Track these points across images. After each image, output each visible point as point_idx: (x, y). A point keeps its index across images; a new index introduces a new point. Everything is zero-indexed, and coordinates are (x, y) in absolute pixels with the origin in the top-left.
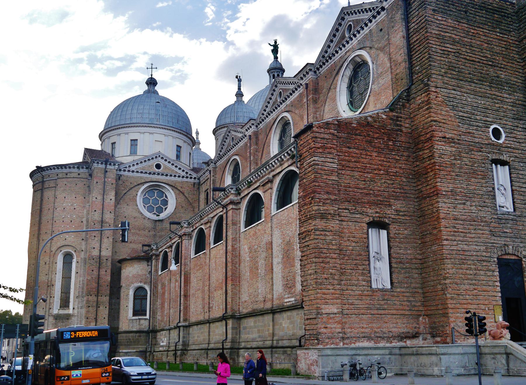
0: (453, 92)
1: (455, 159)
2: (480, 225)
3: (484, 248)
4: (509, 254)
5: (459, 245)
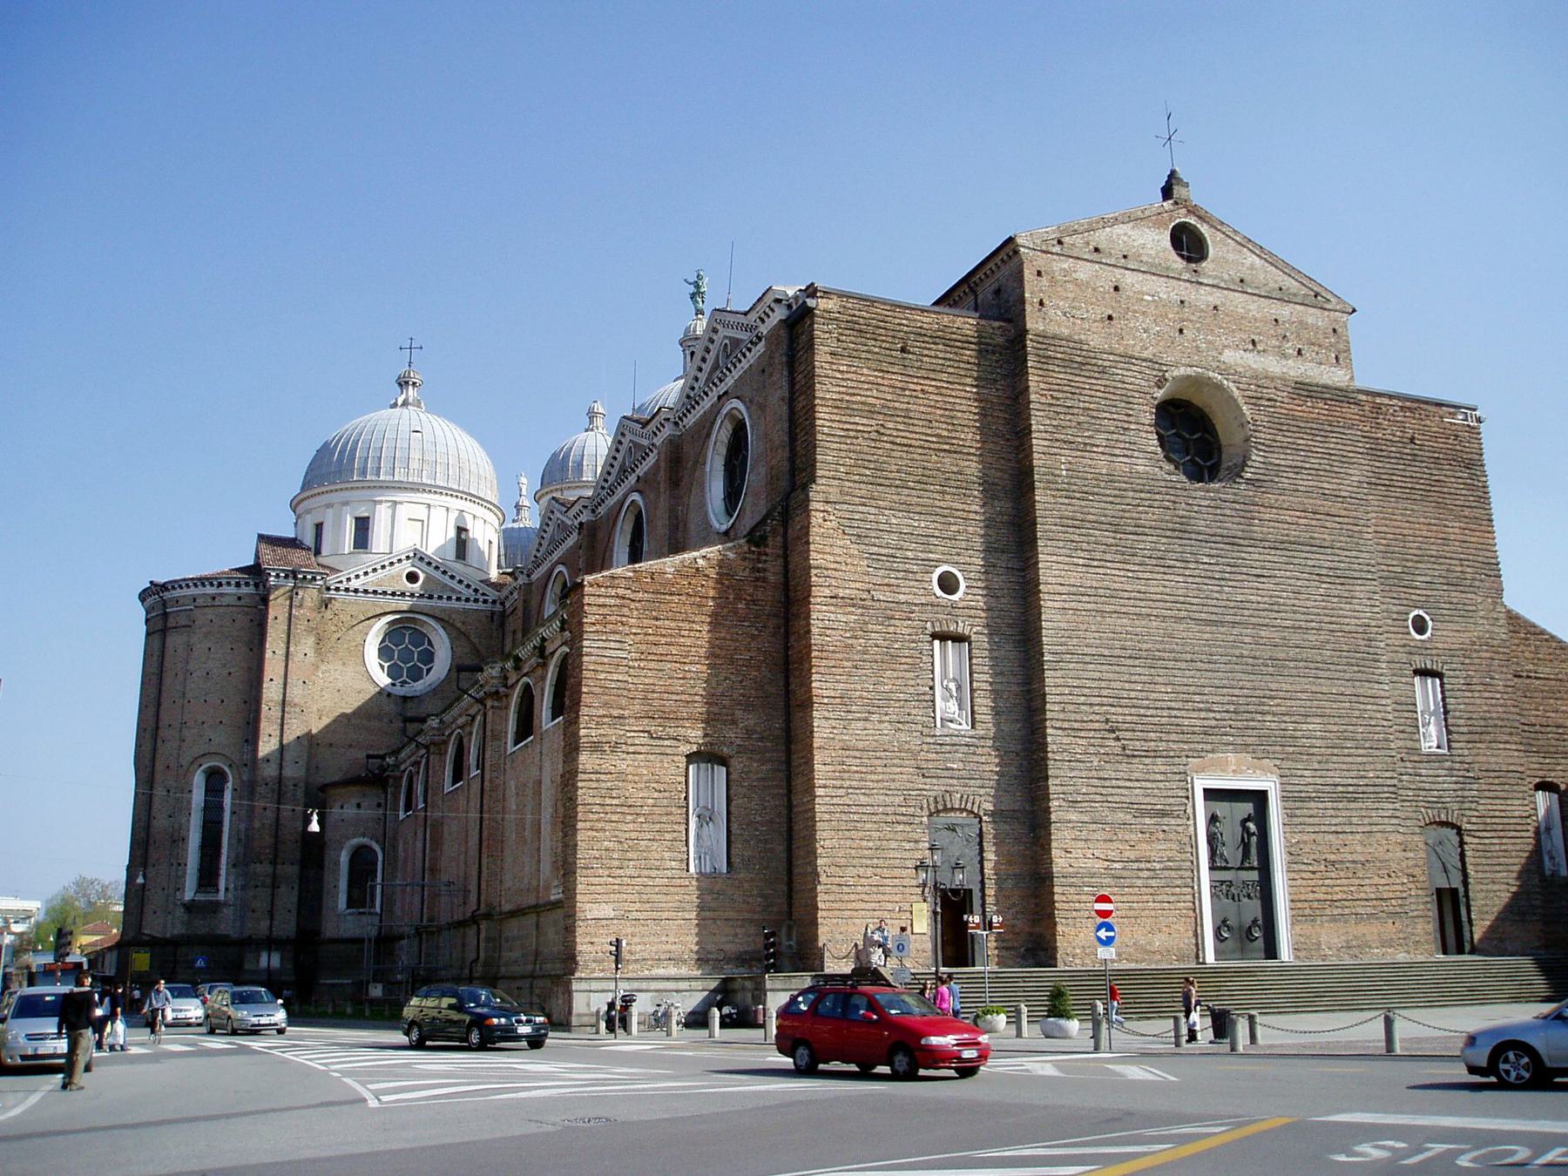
5: (850, 796)
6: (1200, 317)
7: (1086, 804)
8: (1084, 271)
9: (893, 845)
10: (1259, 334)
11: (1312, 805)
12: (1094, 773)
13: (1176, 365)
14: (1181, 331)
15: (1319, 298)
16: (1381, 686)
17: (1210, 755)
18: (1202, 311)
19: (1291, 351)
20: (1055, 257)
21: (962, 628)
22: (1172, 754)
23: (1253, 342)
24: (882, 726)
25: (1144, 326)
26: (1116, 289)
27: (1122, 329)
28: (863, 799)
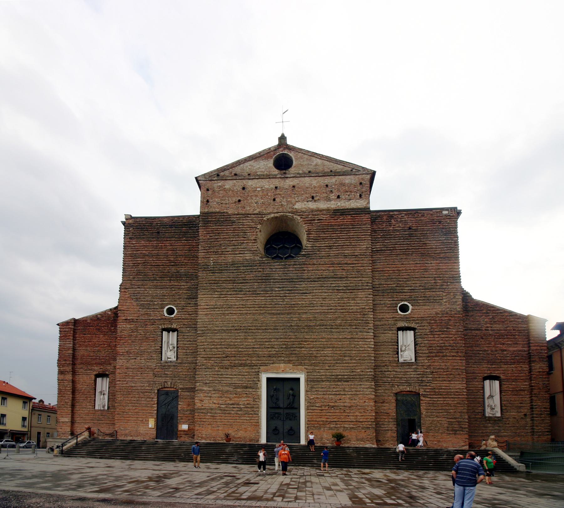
0: (138, 289)
1: (132, 332)
2: (146, 371)
3: (148, 384)
4: (166, 387)
6: (285, 192)
7: (211, 384)
8: (228, 185)
9: (143, 399)
10: (316, 193)
11: (324, 383)
12: (216, 373)
13: (270, 214)
14: (274, 200)
15: (354, 170)
16: (368, 334)
17: (271, 365)
18: (287, 189)
19: (333, 197)
20: (216, 182)
21: (174, 326)
22: (253, 365)
23: (313, 197)
24: (141, 361)
25: (255, 201)
26: (244, 188)
27: (244, 204)
28: (133, 385)
